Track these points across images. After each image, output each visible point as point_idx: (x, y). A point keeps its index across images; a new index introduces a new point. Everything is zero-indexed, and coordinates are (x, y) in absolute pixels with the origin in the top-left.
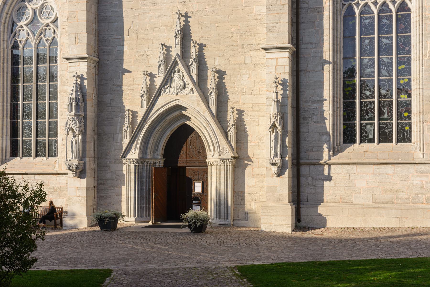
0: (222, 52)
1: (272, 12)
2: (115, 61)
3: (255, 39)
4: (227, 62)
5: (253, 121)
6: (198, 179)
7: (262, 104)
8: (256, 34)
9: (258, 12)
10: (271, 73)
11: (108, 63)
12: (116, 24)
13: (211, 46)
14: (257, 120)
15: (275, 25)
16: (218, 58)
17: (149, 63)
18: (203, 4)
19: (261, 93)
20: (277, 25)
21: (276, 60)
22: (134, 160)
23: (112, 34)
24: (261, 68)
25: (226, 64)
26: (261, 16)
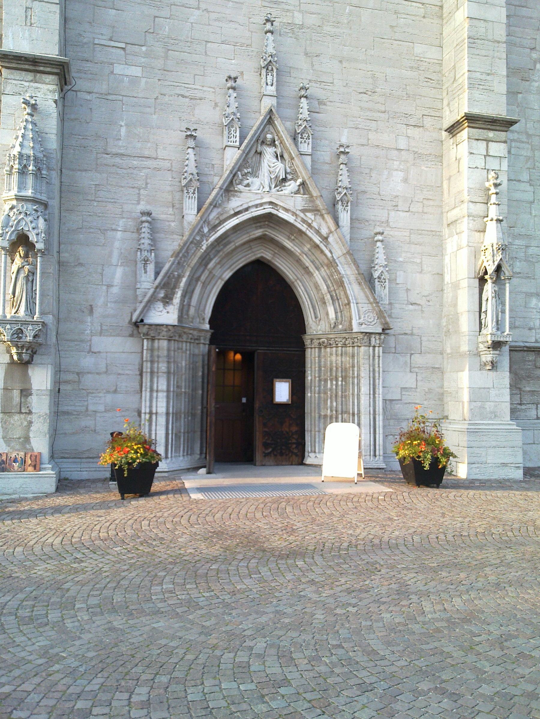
0: (354, 119)
1: (478, 52)
2: (110, 97)
3: (417, 106)
4: (364, 142)
5: (411, 262)
6: (283, 376)
7: (428, 231)
8: (417, 97)
9: (421, 56)
10: (476, 168)
11: (88, 97)
12: (113, 12)
13: (332, 104)
14: (418, 261)
15: (484, 77)
16: (346, 131)
17: (196, 116)
18: (315, 16)
19: (426, 210)
20: (488, 78)
21: (485, 143)
22: (170, 328)
23: (102, 34)
24: (426, 162)
25: (363, 145)
26: (426, 64)
